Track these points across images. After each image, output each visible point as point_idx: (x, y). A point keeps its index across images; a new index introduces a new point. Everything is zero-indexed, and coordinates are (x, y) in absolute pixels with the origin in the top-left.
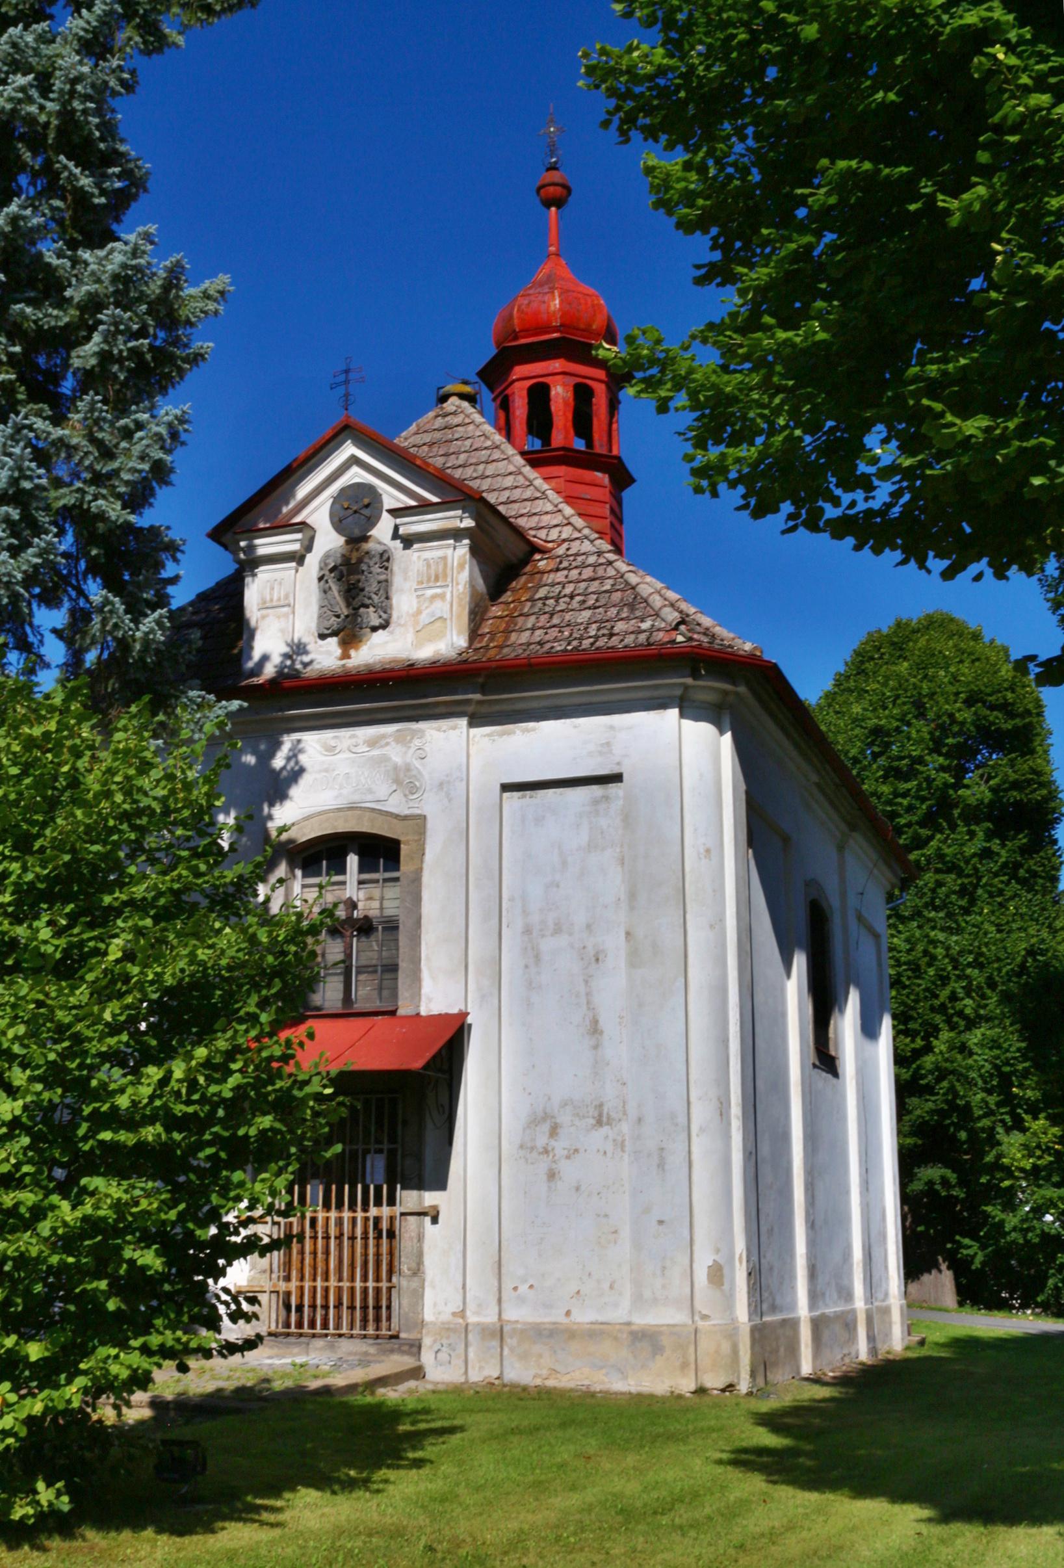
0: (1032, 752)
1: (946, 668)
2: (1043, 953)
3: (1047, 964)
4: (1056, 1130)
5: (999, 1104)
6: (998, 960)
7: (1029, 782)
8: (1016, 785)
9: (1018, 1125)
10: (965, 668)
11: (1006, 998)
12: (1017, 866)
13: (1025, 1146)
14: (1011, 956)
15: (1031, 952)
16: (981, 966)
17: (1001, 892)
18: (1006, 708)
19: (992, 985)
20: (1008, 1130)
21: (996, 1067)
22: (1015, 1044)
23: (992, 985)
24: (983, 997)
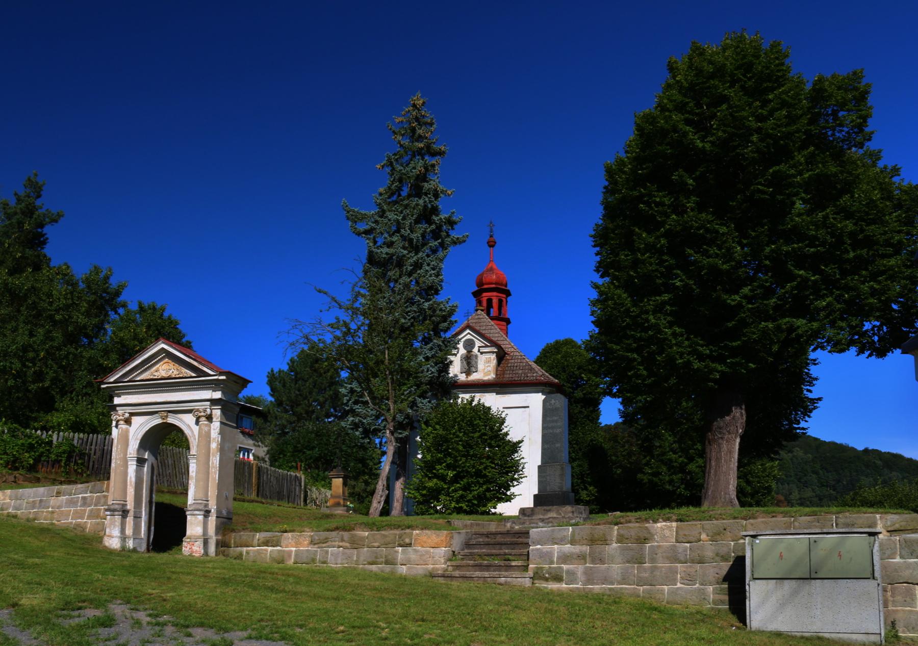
1: (572, 357)
2: (595, 441)
4: (596, 490)
5: (581, 483)
6: (582, 442)
8: (590, 393)
9: (586, 489)
13: (587, 494)
15: (592, 441)
16: (577, 445)
17: (584, 424)
19: (580, 449)
21: (581, 472)
22: (586, 466)
23: (580, 449)
24: (578, 453)
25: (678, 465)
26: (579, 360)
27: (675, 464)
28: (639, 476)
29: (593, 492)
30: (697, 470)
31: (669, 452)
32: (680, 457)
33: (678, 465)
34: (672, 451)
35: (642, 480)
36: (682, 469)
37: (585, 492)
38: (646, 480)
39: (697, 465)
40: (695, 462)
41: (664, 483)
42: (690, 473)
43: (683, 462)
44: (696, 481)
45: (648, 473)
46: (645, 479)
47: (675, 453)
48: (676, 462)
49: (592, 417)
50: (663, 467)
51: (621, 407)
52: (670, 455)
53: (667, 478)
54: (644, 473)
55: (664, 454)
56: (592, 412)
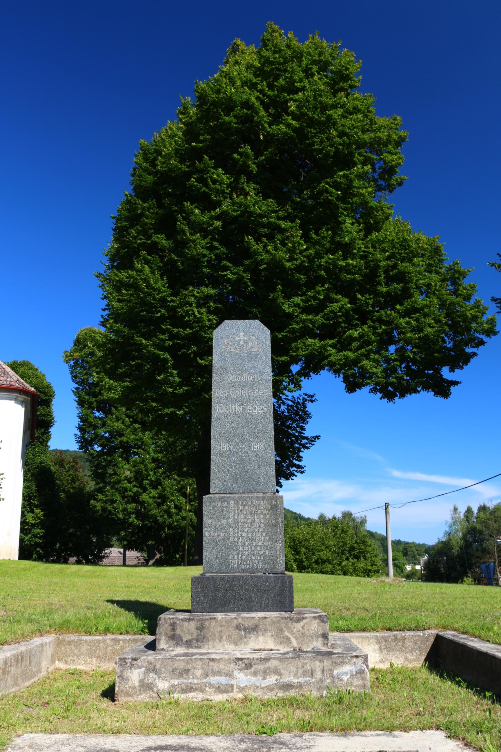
0: (50, 407)
2: (43, 463)
3: (45, 466)
4: (42, 513)
6: (32, 464)
7: (48, 415)
8: (44, 415)
10: (34, 379)
11: (32, 475)
12: (40, 438)
14: (36, 463)
18: (45, 393)
20: (28, 512)
25: (132, 495)
26: (36, 382)
27: (130, 493)
28: (92, 502)
29: (39, 515)
30: (151, 501)
31: (124, 481)
32: (135, 486)
33: (132, 495)
34: (127, 480)
35: (95, 507)
36: (135, 499)
37: (31, 514)
38: (99, 508)
39: (151, 495)
40: (148, 492)
41: (118, 512)
42: (143, 502)
43: (137, 491)
44: (150, 511)
45: (100, 500)
46: (99, 506)
47: (130, 482)
48: (130, 491)
49: (43, 439)
50: (117, 495)
51: (78, 433)
52: (125, 483)
53: (121, 507)
54: (98, 501)
55: (119, 482)
56: (43, 434)
